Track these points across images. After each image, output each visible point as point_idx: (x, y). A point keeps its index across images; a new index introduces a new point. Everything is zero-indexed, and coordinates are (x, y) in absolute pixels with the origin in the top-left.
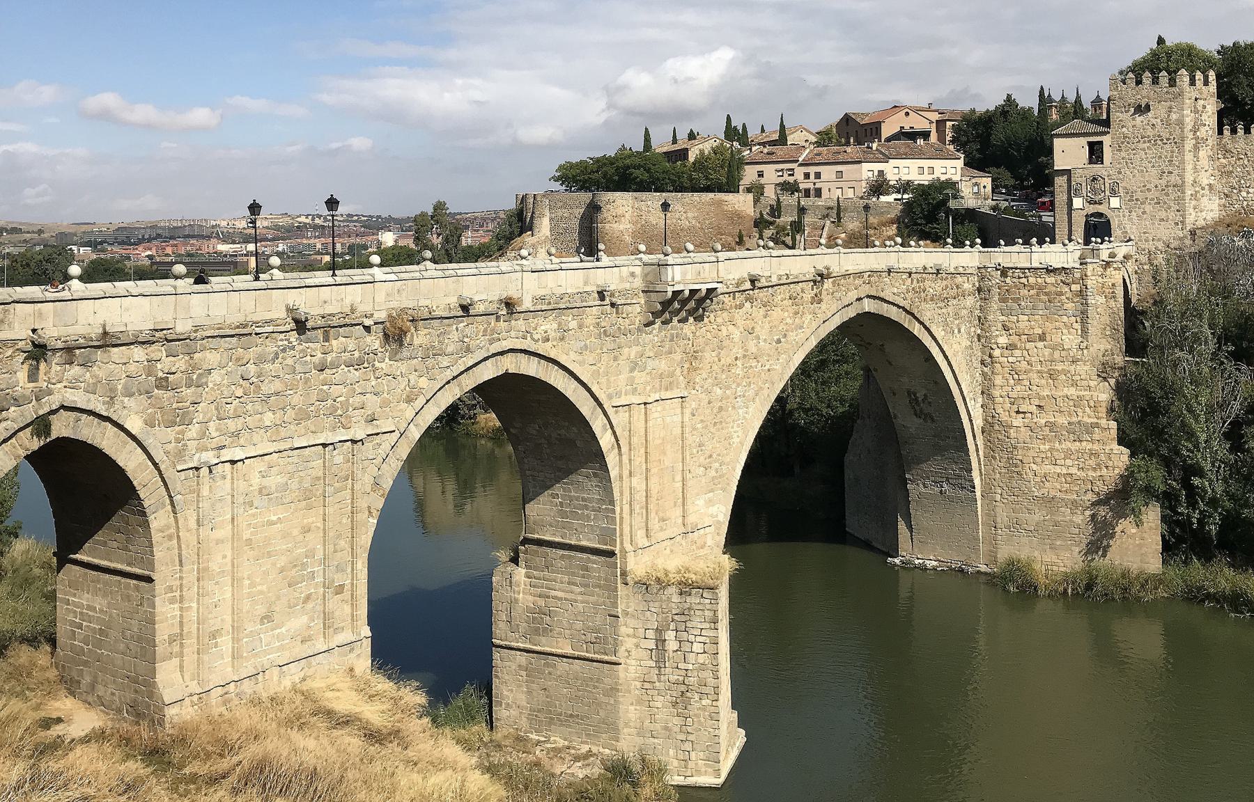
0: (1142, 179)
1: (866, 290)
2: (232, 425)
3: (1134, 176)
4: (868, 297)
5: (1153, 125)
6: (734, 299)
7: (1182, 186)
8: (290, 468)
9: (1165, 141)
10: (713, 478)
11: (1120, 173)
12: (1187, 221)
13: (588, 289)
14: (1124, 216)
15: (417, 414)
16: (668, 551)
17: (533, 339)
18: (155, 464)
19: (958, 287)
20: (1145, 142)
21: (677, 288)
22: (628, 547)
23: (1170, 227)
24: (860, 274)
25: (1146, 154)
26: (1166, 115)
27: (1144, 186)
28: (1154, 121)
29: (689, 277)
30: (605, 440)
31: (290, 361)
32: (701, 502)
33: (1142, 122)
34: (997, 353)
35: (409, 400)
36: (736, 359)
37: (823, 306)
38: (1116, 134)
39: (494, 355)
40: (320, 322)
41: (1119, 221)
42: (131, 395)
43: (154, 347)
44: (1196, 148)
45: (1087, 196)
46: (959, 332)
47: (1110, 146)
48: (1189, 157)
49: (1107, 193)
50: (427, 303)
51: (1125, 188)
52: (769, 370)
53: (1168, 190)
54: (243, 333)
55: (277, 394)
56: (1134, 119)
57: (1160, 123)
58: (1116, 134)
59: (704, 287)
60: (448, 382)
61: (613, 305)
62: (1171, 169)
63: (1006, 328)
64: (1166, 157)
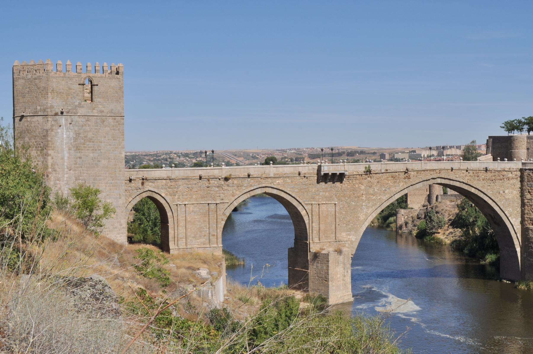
1: (438, 175)
2: (185, 197)
4: (439, 178)
6: (362, 176)
8: (200, 207)
10: (350, 228)
13: (296, 172)
15: (235, 199)
16: (328, 245)
17: (274, 184)
18: (168, 203)
19: (503, 176)
21: (325, 172)
22: (311, 242)
24: (433, 170)
29: (331, 169)
30: (303, 213)
31: (199, 185)
32: (344, 234)
34: (526, 201)
35: (233, 196)
36: (363, 194)
37: (411, 180)
39: (260, 188)
40: (207, 177)
42: (163, 189)
43: (167, 180)
46: (504, 192)
50: (238, 174)
52: (380, 199)
54: (187, 178)
55: (196, 192)
59: (338, 173)
60: (246, 193)
61: (305, 177)
63: (529, 192)
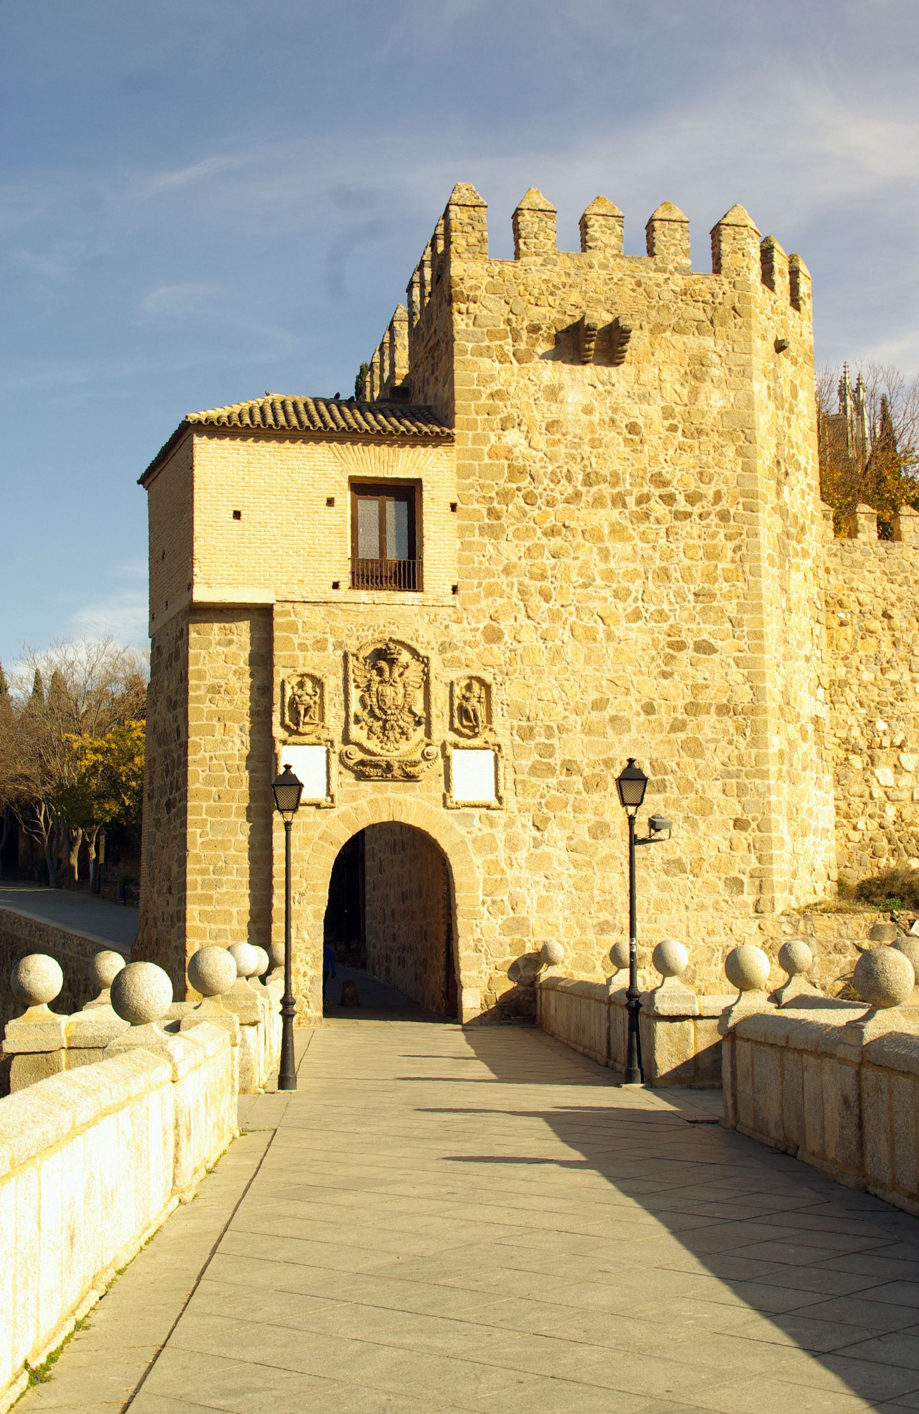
0: (589, 670)
3: (557, 655)
5: (633, 428)
7: (753, 711)
9: (682, 505)
11: (495, 636)
12: (779, 872)
14: (513, 845)
20: (598, 502)
23: (709, 901)
25: (605, 555)
26: (685, 392)
27: (599, 705)
28: (636, 412)
33: (588, 410)
38: (476, 456)
41: (492, 866)
45: (346, 740)
47: (453, 507)
48: (768, 584)
49: (441, 731)
51: (519, 711)
53: (699, 728)
56: (553, 393)
57: (661, 425)
58: (476, 456)
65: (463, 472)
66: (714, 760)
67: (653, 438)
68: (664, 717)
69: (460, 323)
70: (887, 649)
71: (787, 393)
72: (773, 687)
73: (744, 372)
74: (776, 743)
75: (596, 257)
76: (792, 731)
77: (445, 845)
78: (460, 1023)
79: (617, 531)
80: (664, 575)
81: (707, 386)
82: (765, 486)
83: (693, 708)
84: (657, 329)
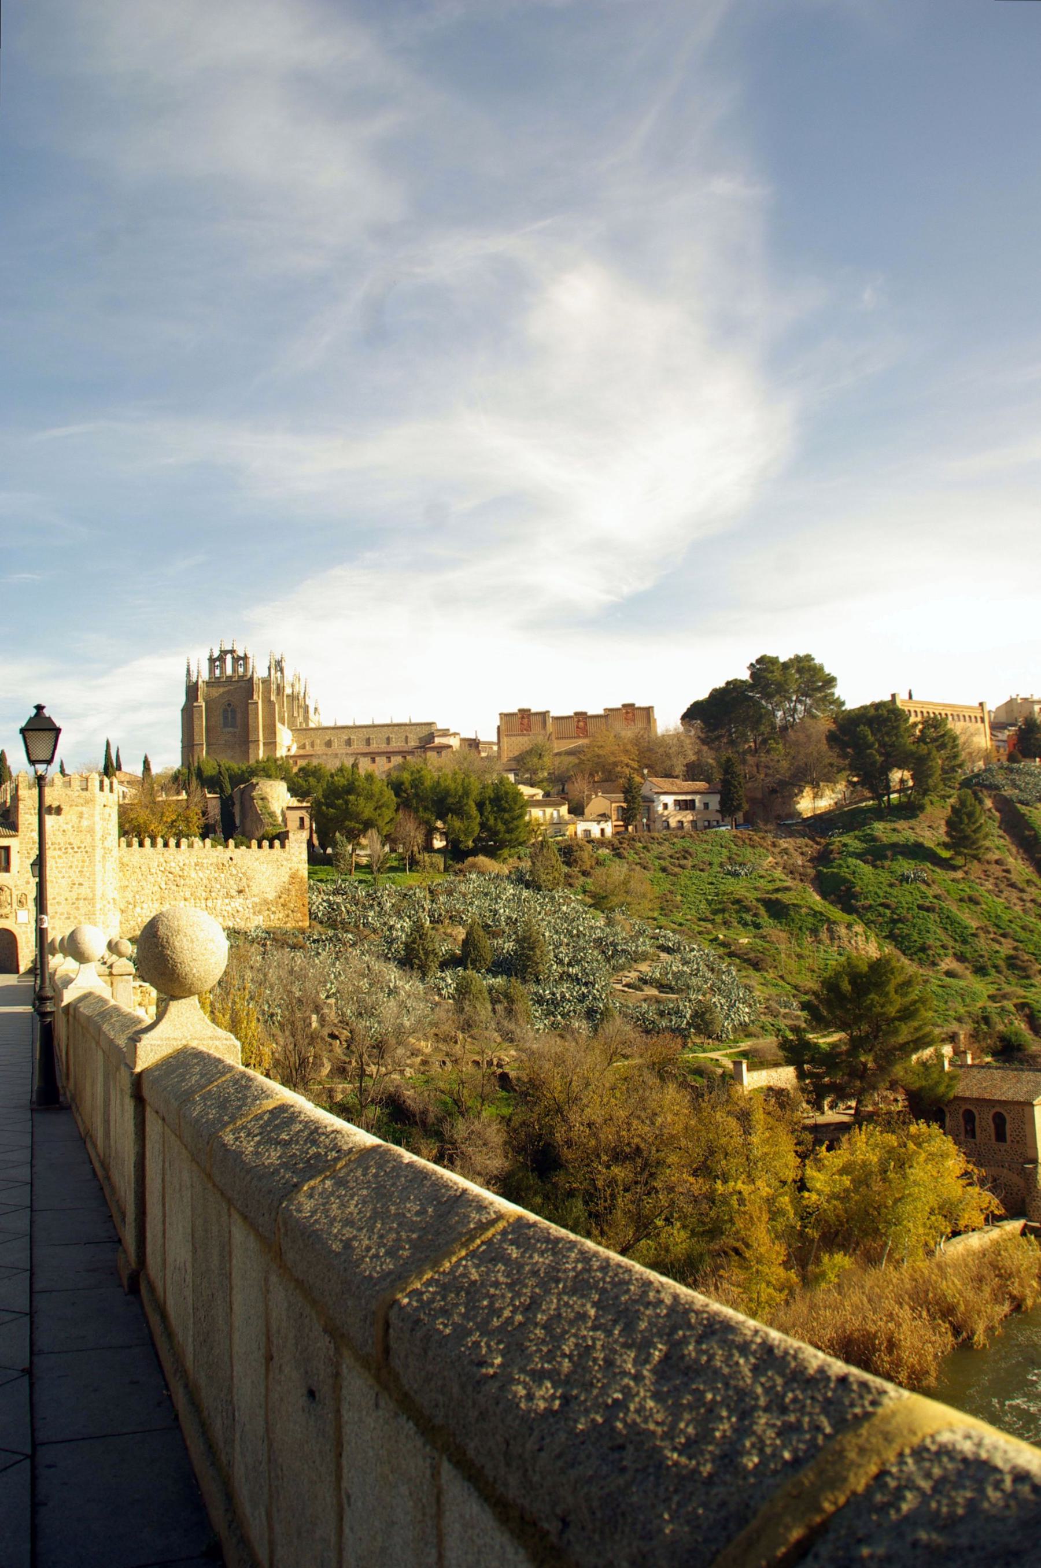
28: (65, 827)
44: (104, 857)
48: (98, 868)
49: (15, 905)
62: (81, 880)
64: (77, 867)
65: (21, 843)
66: (83, 911)
67: (69, 833)
68: (70, 902)
69: (21, 806)
70: (140, 877)
71: (107, 817)
72: (98, 894)
73: (93, 816)
74: (99, 906)
75: (56, 788)
76: (105, 903)
77: (15, 932)
78: (17, 971)
79: (60, 857)
80: (71, 867)
81: (83, 820)
82: (98, 843)
83: (77, 899)
84: (71, 806)
